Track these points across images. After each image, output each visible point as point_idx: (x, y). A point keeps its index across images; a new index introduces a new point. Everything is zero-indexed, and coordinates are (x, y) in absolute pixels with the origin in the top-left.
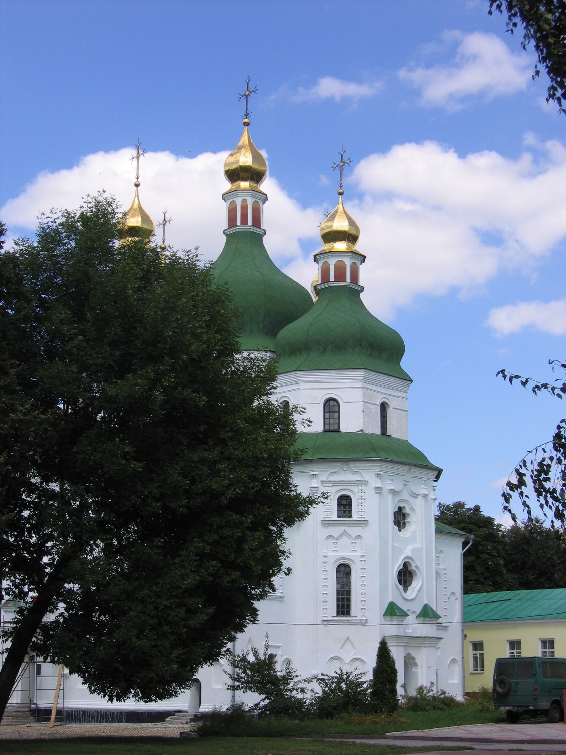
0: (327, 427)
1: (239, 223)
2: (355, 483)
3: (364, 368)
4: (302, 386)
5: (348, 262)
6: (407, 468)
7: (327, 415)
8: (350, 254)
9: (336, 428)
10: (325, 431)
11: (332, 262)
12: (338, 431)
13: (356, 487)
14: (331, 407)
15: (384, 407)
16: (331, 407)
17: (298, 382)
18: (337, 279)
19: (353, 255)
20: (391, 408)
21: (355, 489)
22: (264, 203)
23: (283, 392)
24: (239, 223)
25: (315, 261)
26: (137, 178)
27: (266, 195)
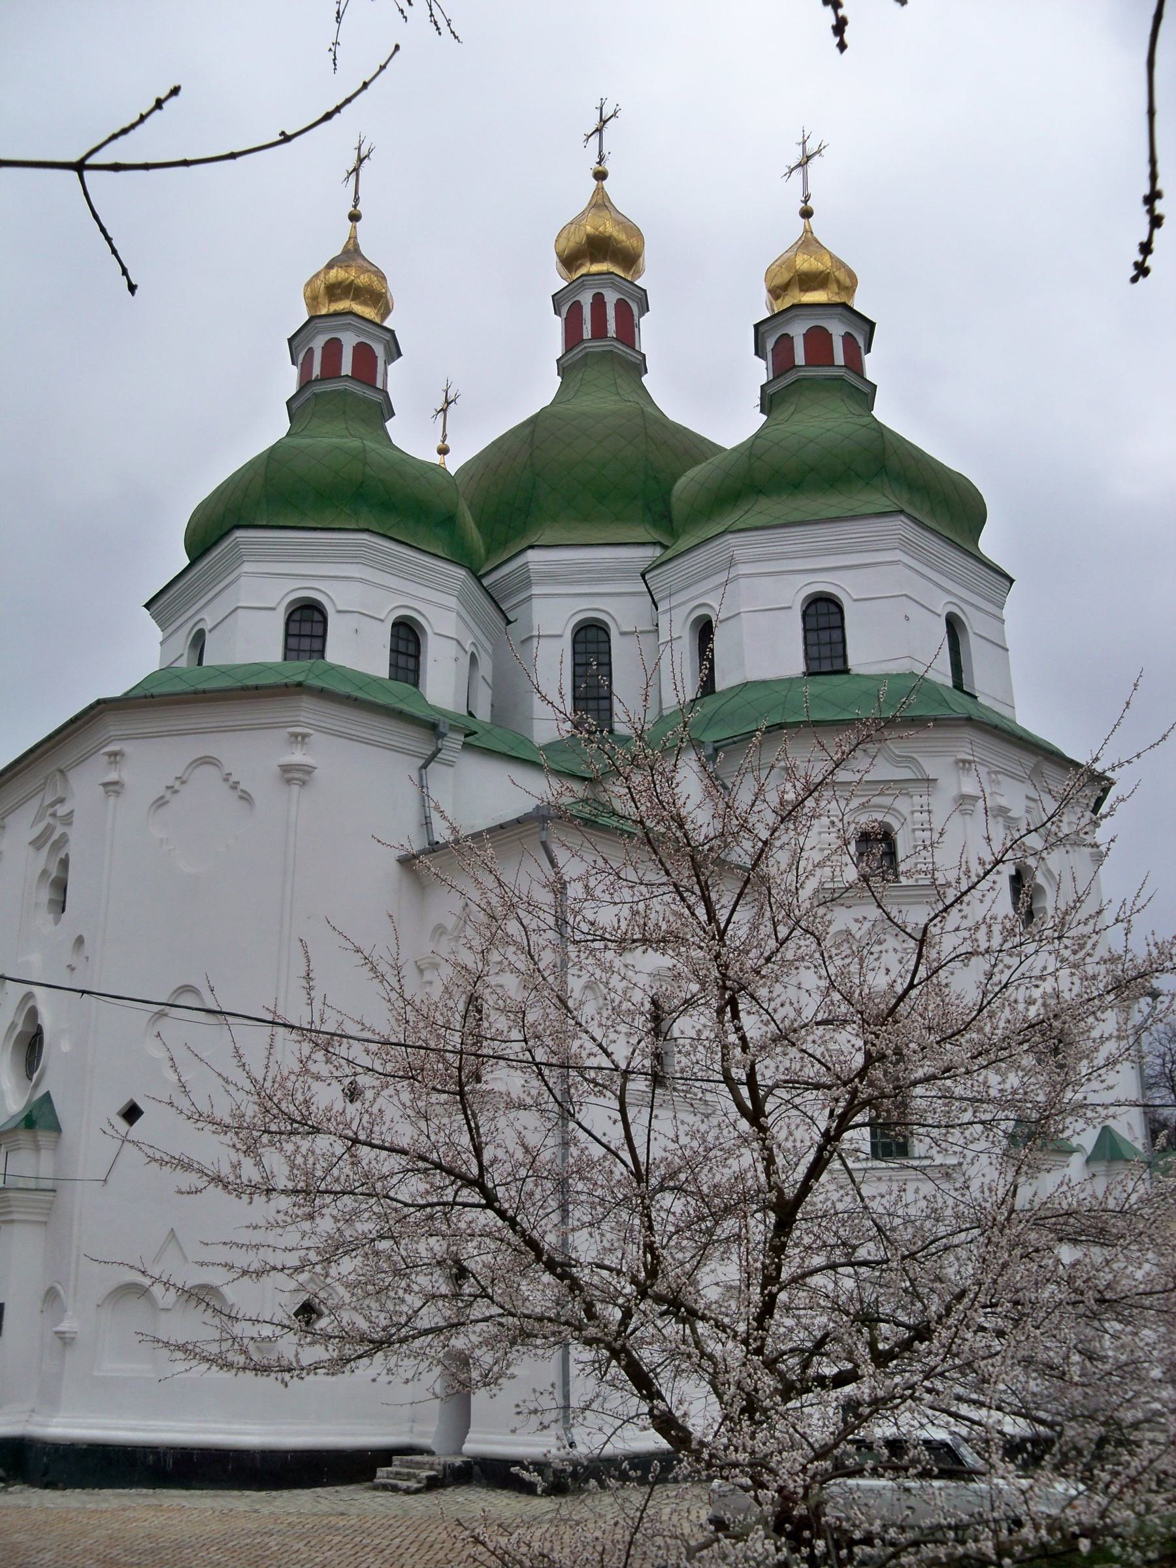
0: (815, 667)
1: (587, 333)
2: (900, 787)
3: (902, 512)
4: (743, 569)
5: (837, 330)
6: (1030, 761)
7: (812, 637)
8: (840, 310)
9: (838, 665)
10: (809, 673)
11: (798, 331)
12: (846, 671)
13: (906, 799)
14: (823, 617)
15: (954, 626)
16: (823, 617)
17: (732, 563)
18: (810, 362)
19: (845, 313)
20: (971, 635)
21: (902, 805)
22: (641, 314)
23: (693, 599)
24: (587, 333)
25: (757, 353)
26: (355, 206)
27: (645, 291)
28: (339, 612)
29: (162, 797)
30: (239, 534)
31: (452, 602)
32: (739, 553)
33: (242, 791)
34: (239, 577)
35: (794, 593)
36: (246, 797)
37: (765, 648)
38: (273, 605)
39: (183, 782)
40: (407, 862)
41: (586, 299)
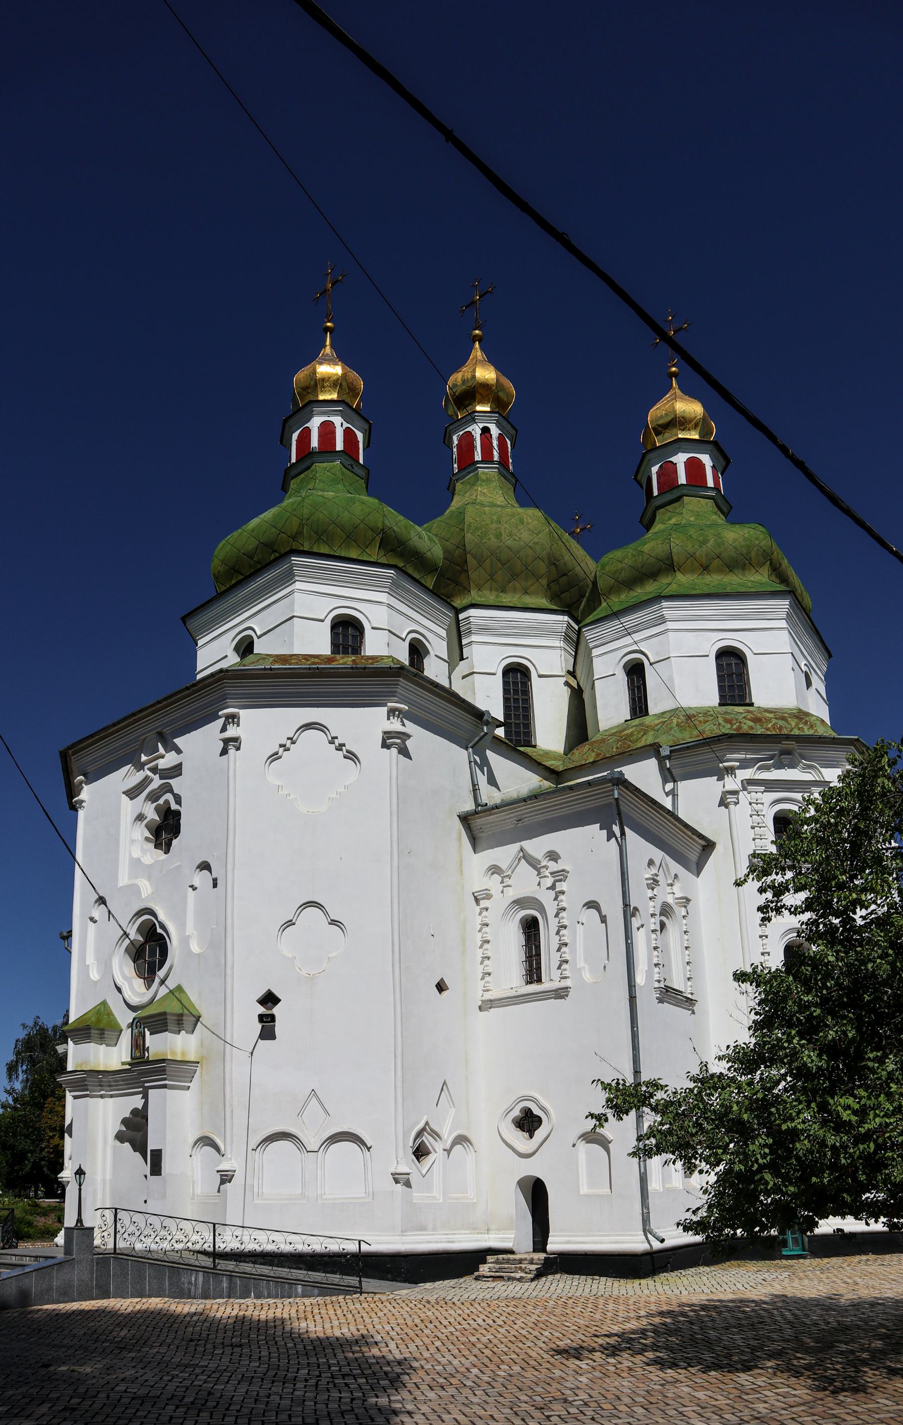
4: (670, 625)
17: (662, 620)
28: (373, 628)
29: (277, 753)
30: (295, 559)
31: (443, 633)
32: (665, 612)
33: (348, 751)
34: (292, 592)
35: (711, 644)
36: (352, 756)
37: (687, 684)
38: (322, 618)
39: (294, 743)
40: (465, 819)
41: (476, 430)
